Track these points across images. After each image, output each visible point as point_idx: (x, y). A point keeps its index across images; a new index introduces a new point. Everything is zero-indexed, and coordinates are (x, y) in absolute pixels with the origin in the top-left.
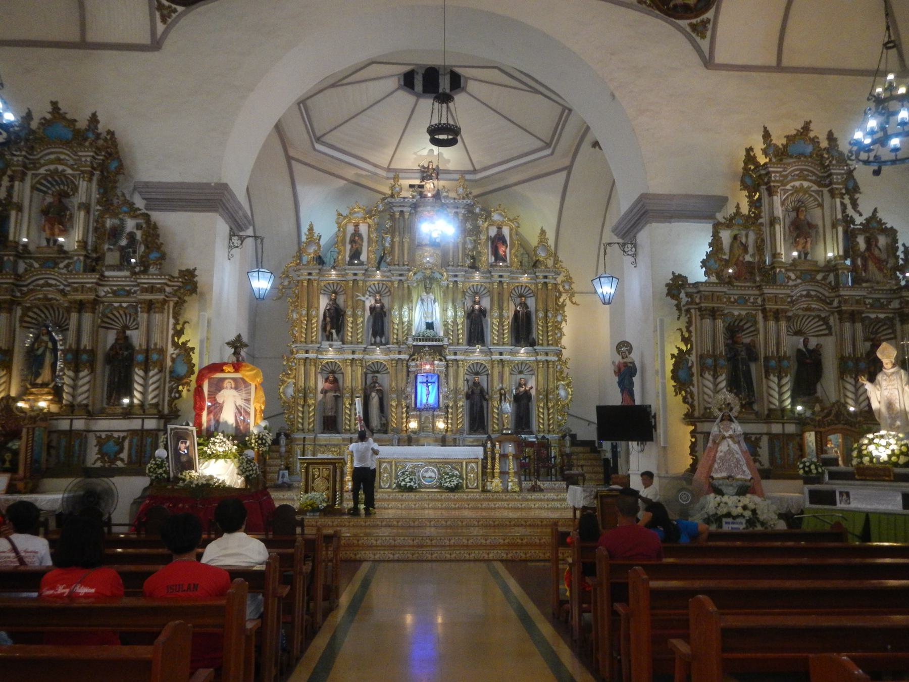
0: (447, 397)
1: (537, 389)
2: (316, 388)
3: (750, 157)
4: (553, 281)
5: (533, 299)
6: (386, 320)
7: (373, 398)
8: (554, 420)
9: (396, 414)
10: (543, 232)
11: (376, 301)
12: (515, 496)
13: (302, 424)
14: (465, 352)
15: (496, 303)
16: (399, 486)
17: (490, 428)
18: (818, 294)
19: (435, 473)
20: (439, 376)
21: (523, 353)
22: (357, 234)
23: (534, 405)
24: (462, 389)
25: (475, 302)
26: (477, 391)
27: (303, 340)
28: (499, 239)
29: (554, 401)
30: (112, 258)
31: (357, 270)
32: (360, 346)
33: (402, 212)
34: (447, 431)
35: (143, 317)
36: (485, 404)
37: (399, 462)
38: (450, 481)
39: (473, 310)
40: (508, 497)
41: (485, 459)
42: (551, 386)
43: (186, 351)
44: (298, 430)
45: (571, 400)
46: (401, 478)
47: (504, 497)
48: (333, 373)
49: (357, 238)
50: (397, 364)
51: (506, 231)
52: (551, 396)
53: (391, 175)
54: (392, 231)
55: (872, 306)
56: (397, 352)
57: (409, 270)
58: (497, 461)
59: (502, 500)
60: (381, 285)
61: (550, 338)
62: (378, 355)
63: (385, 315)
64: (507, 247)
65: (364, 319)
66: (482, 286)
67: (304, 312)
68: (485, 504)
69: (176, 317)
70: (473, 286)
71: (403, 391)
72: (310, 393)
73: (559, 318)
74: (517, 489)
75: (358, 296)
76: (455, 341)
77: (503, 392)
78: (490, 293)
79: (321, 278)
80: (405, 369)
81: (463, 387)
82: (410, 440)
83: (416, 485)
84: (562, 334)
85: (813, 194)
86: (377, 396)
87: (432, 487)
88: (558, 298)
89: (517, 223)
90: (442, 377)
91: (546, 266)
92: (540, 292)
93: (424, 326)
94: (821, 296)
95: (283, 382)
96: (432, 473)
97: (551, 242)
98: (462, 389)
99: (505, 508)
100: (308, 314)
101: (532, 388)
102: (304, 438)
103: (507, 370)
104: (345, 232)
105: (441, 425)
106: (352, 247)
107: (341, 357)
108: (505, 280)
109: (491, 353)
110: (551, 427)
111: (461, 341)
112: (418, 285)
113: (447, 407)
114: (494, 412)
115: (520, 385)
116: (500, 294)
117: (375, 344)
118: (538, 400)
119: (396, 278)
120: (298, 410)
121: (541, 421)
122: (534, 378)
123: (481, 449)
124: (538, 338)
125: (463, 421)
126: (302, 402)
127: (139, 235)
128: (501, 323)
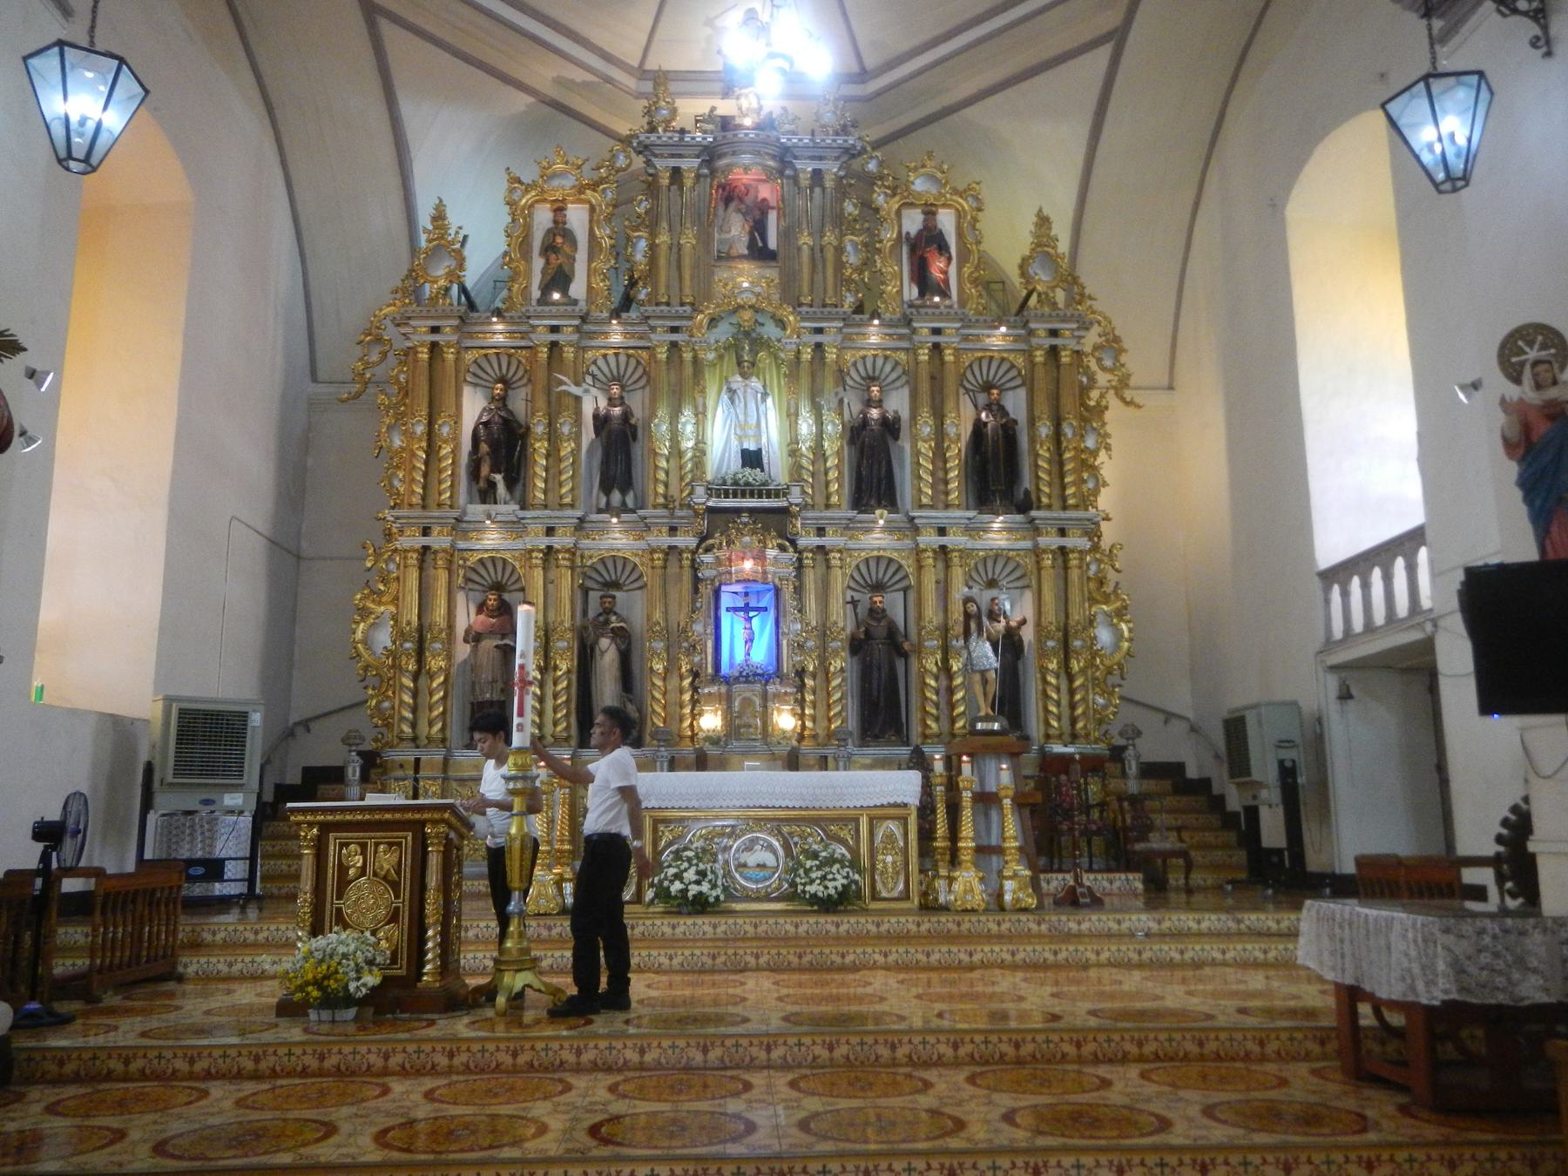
0: (801, 646)
1: (1038, 624)
2: (451, 626)
4: (1072, 344)
5: (1022, 393)
6: (637, 450)
7: (603, 653)
8: (1087, 707)
9: (664, 694)
10: (1043, 221)
11: (611, 402)
12: (1029, 923)
13: (414, 725)
14: (847, 528)
15: (925, 397)
17: (916, 730)
19: (775, 852)
20: (777, 591)
21: (998, 531)
22: (559, 228)
24: (841, 624)
25: (869, 403)
26: (880, 630)
27: (416, 500)
28: (928, 242)
29: (1086, 655)
31: (562, 317)
32: (569, 512)
33: (676, 173)
34: (801, 738)
36: (900, 665)
37: (666, 821)
38: (824, 878)
39: (865, 422)
40: (1005, 926)
41: (926, 810)
42: (1076, 616)
44: (402, 739)
45: (1128, 653)
46: (672, 871)
47: (994, 927)
49: (559, 240)
50: (666, 560)
51: (946, 221)
52: (1077, 643)
53: (648, 87)
56: (665, 529)
58: (967, 814)
59: (989, 938)
60: (623, 359)
61: (1070, 491)
62: (617, 538)
63: (635, 438)
64: (949, 259)
65: (579, 445)
66: (886, 358)
67: (420, 429)
68: (939, 953)
70: (864, 358)
72: (434, 639)
73: (1090, 442)
74: (1032, 902)
75: (565, 384)
76: (820, 500)
77: (973, 608)
79: (469, 343)
80: (687, 575)
81: (843, 620)
83: (719, 891)
84: (1100, 484)
86: (613, 646)
87: (767, 898)
88: (1084, 391)
89: (976, 198)
90: (788, 592)
92: (1040, 373)
93: (735, 463)
95: (364, 613)
96: (764, 854)
97: (1063, 246)
98: (841, 624)
99: (1002, 965)
100: (430, 434)
101: (1024, 622)
102: (417, 761)
103: (958, 574)
104: (528, 228)
105: (785, 720)
106: (548, 262)
107: (519, 544)
108: (950, 339)
109: (916, 530)
110: (1080, 725)
111: (835, 499)
112: (721, 357)
113: (801, 673)
114: (925, 684)
116: (937, 380)
117: (608, 509)
118: (1043, 654)
119: (661, 339)
120: (402, 686)
121: (1053, 709)
122: (1028, 597)
123: (913, 778)
124: (1038, 490)
125: (845, 712)
126: (412, 667)
128: (940, 455)
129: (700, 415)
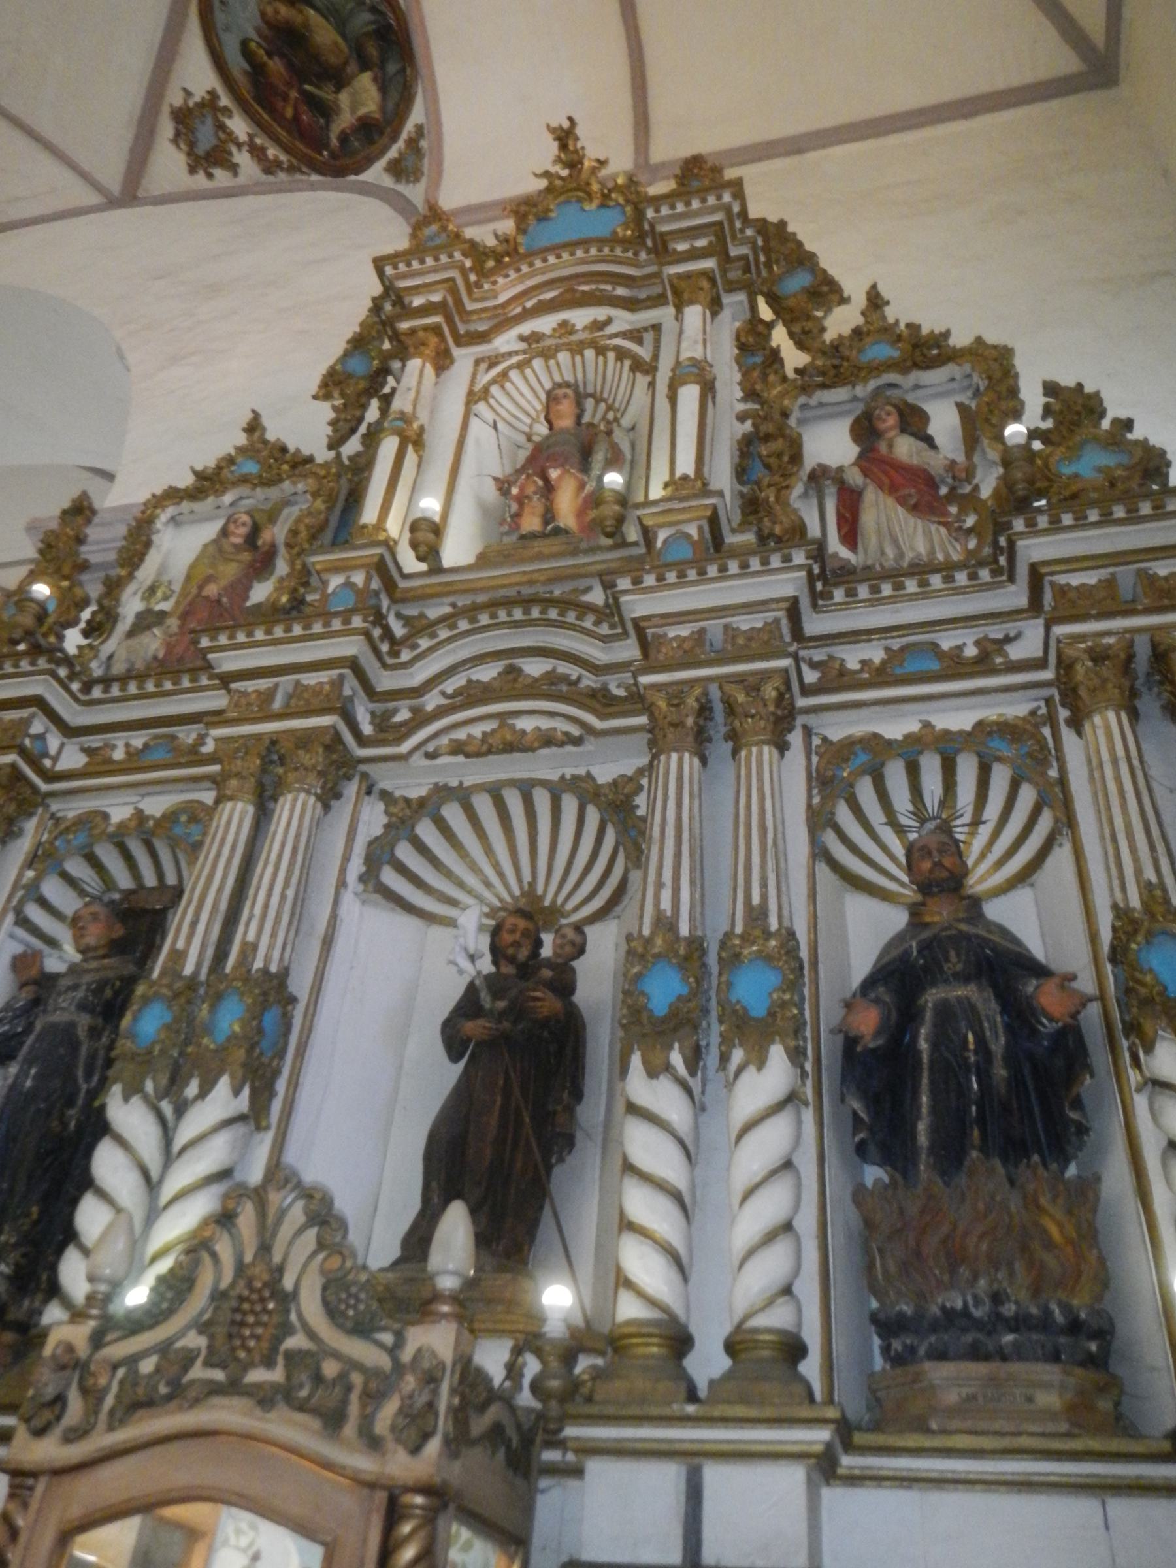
18: (564, 668)
55: (881, 676)
85: (618, 342)
94: (574, 671)
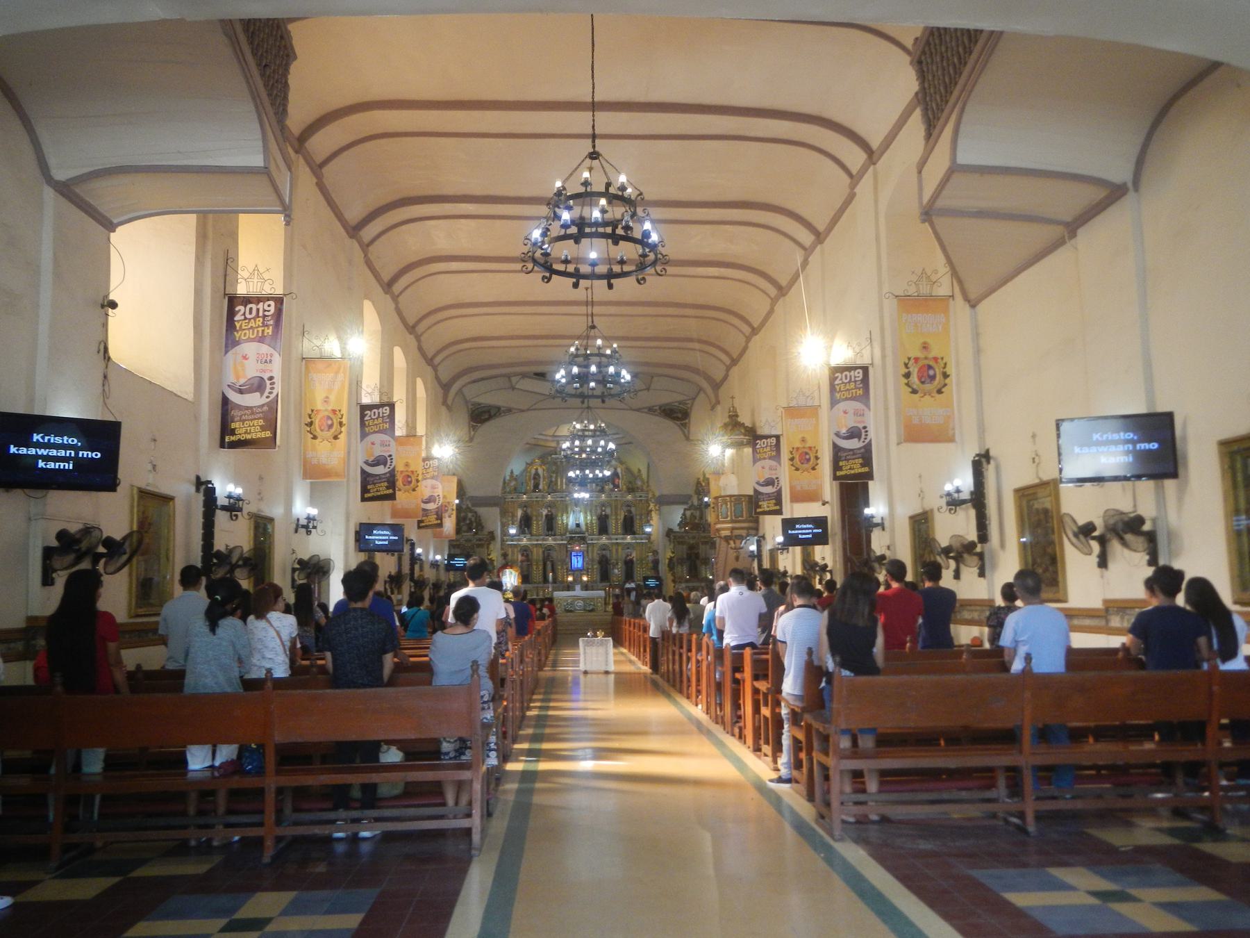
3: (698, 483)
10: (639, 471)
11: (549, 511)
16: (565, 610)
22: (537, 474)
23: (635, 565)
25: (603, 511)
30: (465, 528)
35: (478, 550)
39: (601, 515)
43: (492, 561)
48: (525, 551)
51: (619, 470)
54: (556, 472)
57: (567, 496)
62: (550, 541)
69: (488, 548)
71: (564, 561)
78: (611, 505)
81: (597, 558)
82: (569, 587)
90: (585, 553)
91: (642, 490)
93: (575, 526)
96: (581, 603)
97: (644, 476)
103: (620, 548)
104: (530, 472)
105: (585, 578)
115: (628, 556)
116: (616, 507)
125: (597, 577)
127: (473, 519)
128: (617, 523)
129: (568, 518)
